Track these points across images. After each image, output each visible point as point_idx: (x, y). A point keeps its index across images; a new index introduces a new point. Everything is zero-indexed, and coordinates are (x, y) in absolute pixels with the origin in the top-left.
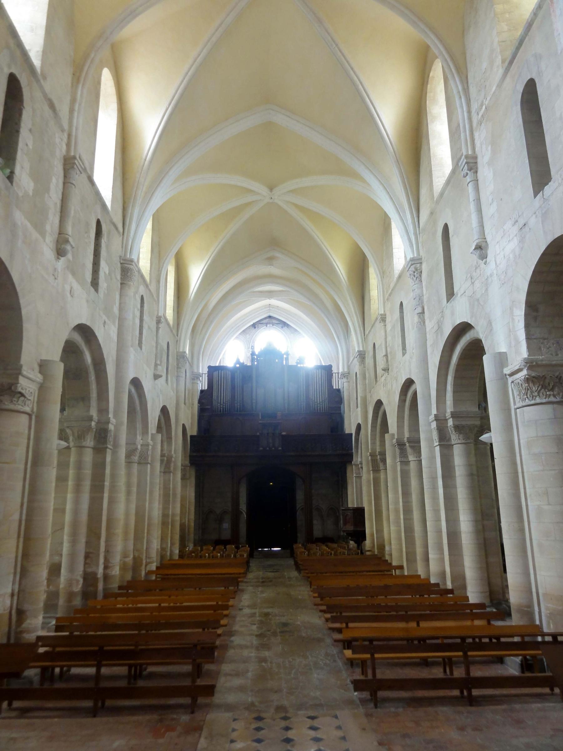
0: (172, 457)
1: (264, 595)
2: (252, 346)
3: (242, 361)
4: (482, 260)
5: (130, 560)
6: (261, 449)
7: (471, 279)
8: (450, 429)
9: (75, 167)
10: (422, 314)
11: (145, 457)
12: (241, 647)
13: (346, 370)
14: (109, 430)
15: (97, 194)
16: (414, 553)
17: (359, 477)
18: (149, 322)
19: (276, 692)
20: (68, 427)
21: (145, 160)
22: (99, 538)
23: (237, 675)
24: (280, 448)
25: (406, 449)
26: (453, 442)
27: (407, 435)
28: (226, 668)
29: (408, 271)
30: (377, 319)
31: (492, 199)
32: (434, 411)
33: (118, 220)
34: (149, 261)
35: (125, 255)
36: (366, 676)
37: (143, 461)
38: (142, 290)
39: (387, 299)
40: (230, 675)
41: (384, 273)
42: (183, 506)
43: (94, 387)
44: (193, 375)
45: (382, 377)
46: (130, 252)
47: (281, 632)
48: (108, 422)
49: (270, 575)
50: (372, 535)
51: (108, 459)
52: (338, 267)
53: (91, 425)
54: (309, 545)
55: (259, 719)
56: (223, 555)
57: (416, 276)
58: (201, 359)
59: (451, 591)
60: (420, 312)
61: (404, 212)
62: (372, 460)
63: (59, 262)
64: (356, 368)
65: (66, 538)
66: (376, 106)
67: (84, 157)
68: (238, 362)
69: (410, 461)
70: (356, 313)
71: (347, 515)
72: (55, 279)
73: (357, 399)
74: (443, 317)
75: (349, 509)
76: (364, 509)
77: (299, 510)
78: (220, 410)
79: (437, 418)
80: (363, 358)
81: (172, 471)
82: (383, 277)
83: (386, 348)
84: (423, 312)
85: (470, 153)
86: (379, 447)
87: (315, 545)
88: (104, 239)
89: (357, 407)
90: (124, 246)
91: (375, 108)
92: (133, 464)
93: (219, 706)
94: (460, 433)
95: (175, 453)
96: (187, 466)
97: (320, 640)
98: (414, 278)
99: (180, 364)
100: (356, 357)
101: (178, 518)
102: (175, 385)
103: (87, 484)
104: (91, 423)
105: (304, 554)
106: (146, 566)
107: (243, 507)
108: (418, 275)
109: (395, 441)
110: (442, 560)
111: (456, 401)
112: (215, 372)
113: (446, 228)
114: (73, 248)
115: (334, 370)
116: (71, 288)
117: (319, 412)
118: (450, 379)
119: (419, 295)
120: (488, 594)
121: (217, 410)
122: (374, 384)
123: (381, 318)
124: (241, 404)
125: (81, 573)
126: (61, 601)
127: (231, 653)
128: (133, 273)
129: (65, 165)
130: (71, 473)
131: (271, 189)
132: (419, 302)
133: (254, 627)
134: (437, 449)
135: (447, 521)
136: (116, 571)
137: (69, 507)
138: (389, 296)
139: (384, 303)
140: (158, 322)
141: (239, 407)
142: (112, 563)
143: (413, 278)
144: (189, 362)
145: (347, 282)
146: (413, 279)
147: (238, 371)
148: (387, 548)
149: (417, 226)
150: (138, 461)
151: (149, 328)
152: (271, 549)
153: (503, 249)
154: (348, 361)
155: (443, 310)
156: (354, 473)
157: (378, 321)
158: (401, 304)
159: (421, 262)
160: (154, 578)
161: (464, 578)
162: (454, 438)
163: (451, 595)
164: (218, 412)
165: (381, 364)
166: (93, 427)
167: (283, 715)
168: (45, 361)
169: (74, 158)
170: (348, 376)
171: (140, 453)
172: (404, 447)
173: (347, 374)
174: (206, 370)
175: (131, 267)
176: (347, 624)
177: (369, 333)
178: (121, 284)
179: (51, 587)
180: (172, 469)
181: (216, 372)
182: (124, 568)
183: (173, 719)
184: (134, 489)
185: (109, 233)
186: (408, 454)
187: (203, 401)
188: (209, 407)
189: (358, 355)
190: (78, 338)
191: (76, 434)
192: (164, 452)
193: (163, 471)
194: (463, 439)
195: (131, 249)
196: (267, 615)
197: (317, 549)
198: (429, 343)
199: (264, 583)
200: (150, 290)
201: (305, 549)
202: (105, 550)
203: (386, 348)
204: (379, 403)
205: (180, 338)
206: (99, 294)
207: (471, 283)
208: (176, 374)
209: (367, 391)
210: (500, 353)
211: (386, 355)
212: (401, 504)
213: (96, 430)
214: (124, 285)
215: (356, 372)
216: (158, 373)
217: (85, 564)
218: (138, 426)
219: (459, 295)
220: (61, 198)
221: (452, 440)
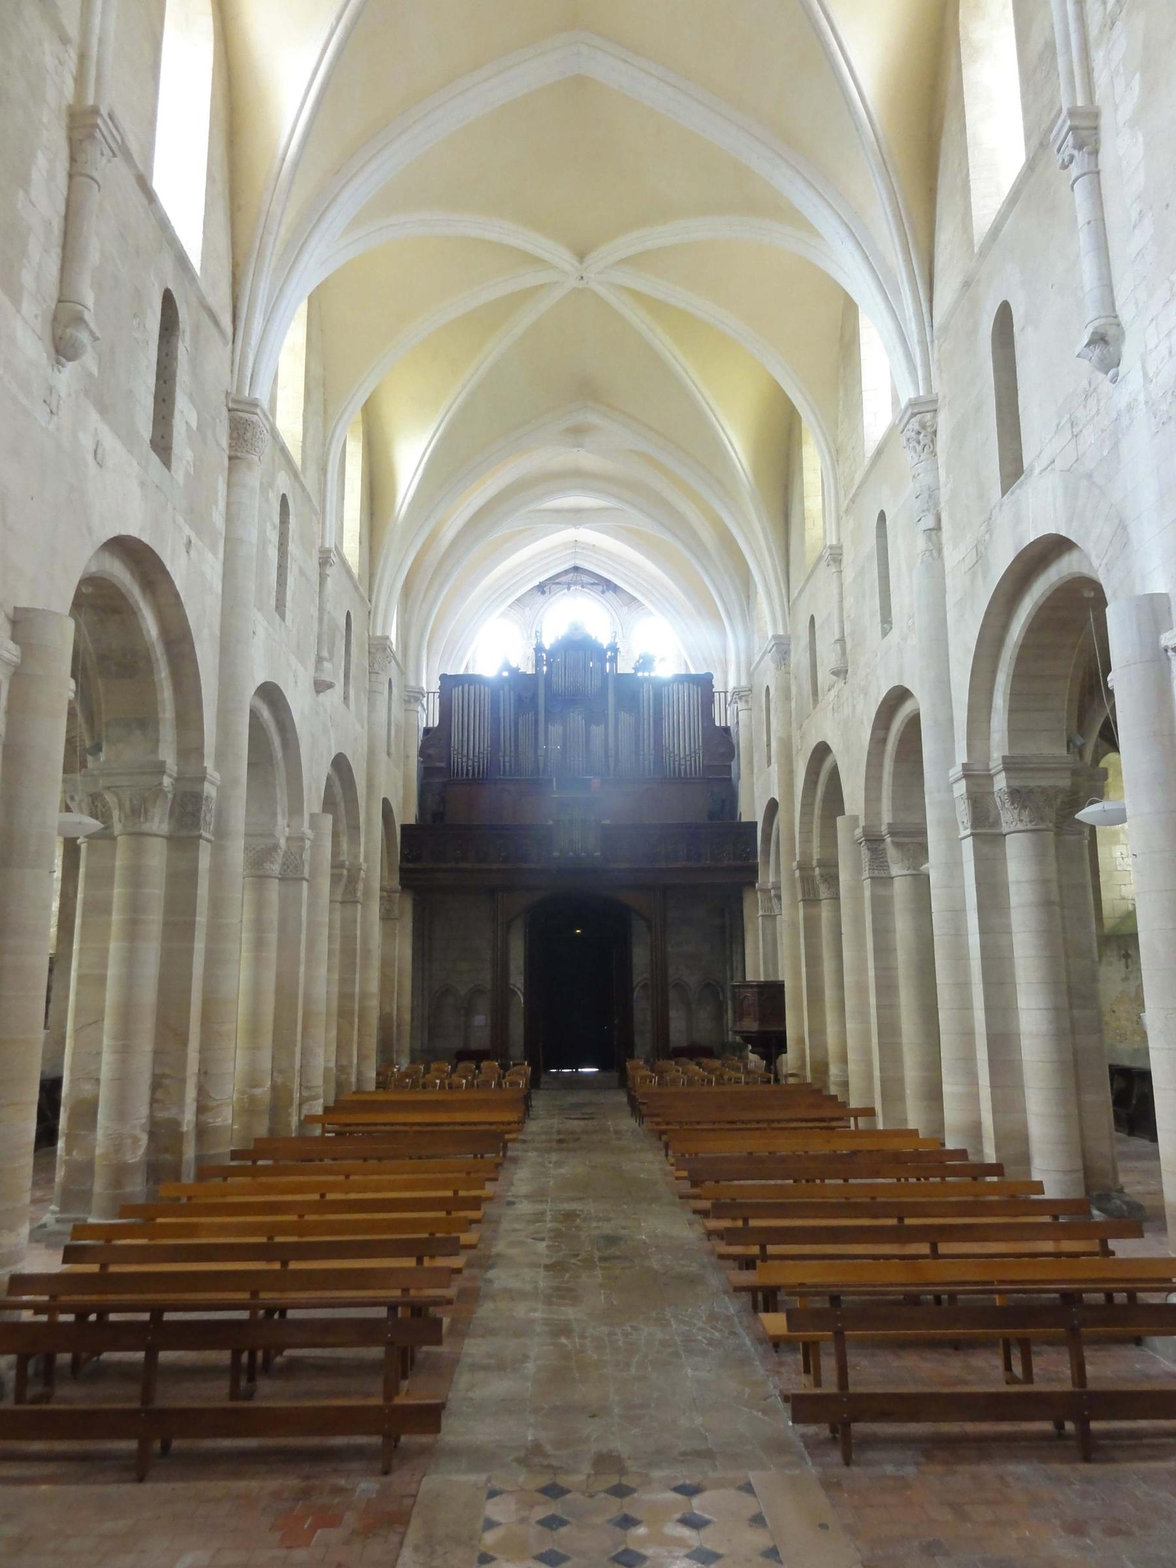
0: (361, 869)
1: (563, 1171)
2: (537, 632)
3: (514, 666)
4: (1107, 373)
5: (263, 1092)
6: (556, 854)
7: (1072, 425)
8: (1000, 797)
9: (98, 135)
10: (935, 532)
11: (296, 865)
12: (511, 1295)
13: (744, 683)
14: (205, 794)
15: (163, 225)
16: (900, 1081)
17: (771, 918)
18: (301, 559)
19: (593, 1416)
20: (108, 788)
21: (283, 160)
22: (185, 1043)
23: (501, 1367)
25: (884, 849)
26: (1005, 829)
27: (886, 818)
28: (474, 1348)
29: (902, 432)
30: (820, 558)
31: (1141, 211)
32: (961, 757)
33: (220, 300)
34: (301, 420)
35: (239, 389)
36: (818, 1383)
37: (291, 876)
38: (283, 483)
39: (847, 511)
40: (485, 1368)
41: (836, 453)
42: (385, 979)
43: (167, 695)
44: (406, 693)
45: (829, 690)
46: (251, 385)
47: (602, 1259)
48: (202, 778)
49: (577, 1125)
50: (801, 1041)
51: (204, 862)
52: (731, 444)
53: (161, 784)
54: (662, 1063)
55: (554, 1491)
56: (474, 1084)
57: (922, 443)
58: (424, 658)
59: (997, 1169)
60: (931, 527)
61: (898, 292)
62: (802, 878)
63: (60, 371)
64: (769, 677)
65: (106, 1041)
66: (835, 22)
67: (126, 124)
68: (507, 667)
69: (892, 878)
70: (770, 550)
71: (746, 997)
72: (52, 412)
73: (769, 745)
74: (989, 531)
75: (748, 985)
76: (783, 986)
77: (638, 988)
78: (467, 770)
79: (968, 773)
80: (785, 653)
81: (361, 900)
82: (838, 461)
83: (842, 622)
84: (938, 528)
85: (1080, 103)
86: (819, 849)
87: (674, 1063)
88: (183, 341)
89: (769, 763)
90: (236, 366)
91: (833, 28)
92: (271, 879)
93: (454, 1453)
94: (1024, 807)
95: (366, 859)
96: (395, 892)
97: (692, 1281)
98: (917, 445)
99: (376, 665)
100: (768, 650)
101: (374, 1003)
102: (365, 714)
103: (155, 919)
104: (162, 778)
105: (651, 1082)
106: (300, 1105)
107: (517, 980)
108: (927, 441)
109: (859, 832)
110: (974, 1098)
111: (1015, 732)
113: (1004, 314)
114: (96, 339)
115: (718, 686)
116: (98, 444)
118: (1002, 680)
119: (929, 488)
120: (1081, 1175)
121: (460, 771)
122: (812, 707)
123: (831, 554)
124: (513, 758)
125: (144, 1121)
126: (99, 1186)
127: (485, 1310)
128: (259, 433)
129: (71, 128)
130: (118, 892)
131: (581, 256)
132: (928, 502)
133: (542, 1246)
134: (968, 846)
135: (989, 1009)
136: (225, 1118)
137: (113, 971)
138: (851, 503)
139: (838, 519)
140: (324, 562)
142: (216, 1100)
143: (914, 447)
144: (398, 664)
145: (751, 478)
146: (916, 452)
147: (506, 688)
148: (834, 1070)
149: (926, 324)
150: (280, 874)
151: (302, 572)
153: (1168, 335)
154: (749, 663)
155: (991, 513)
156: (760, 908)
157: (823, 564)
158: (882, 516)
159: (934, 408)
160: (318, 1132)
161: (1025, 1139)
162: (1009, 818)
163: (995, 1179)
164: (462, 774)
165: (828, 658)
166: (165, 789)
167: (614, 1480)
168: (26, 610)
169: (95, 111)
171: (284, 855)
172: (879, 846)
174: (435, 686)
175: (255, 418)
176: (763, 1248)
177: (800, 594)
178: (230, 458)
179: (75, 1153)
180: (359, 894)
182: (249, 1108)
183: (337, 1491)
184: (273, 937)
185: (197, 330)
186: (889, 861)
187: (431, 751)
188: (443, 765)
189: (773, 646)
190: (119, 572)
191: (127, 804)
192: (342, 858)
193: (340, 900)
194: (1031, 821)
195: (252, 375)
196: (570, 1216)
197: (678, 1071)
198: (951, 600)
199: (564, 1142)
200: (303, 489)
201: (652, 1071)
202: (199, 1070)
203: (842, 622)
204: (822, 751)
205: (376, 607)
206: (172, 472)
207: (1070, 437)
208: (367, 687)
209: (794, 725)
210: (1152, 597)
211: (842, 640)
212: (871, 973)
213: (175, 796)
214: (236, 461)
215: (768, 687)
216: (326, 677)
217: (153, 1101)
218: (279, 796)
219: (1037, 471)
220: (63, 214)
221: (1004, 825)
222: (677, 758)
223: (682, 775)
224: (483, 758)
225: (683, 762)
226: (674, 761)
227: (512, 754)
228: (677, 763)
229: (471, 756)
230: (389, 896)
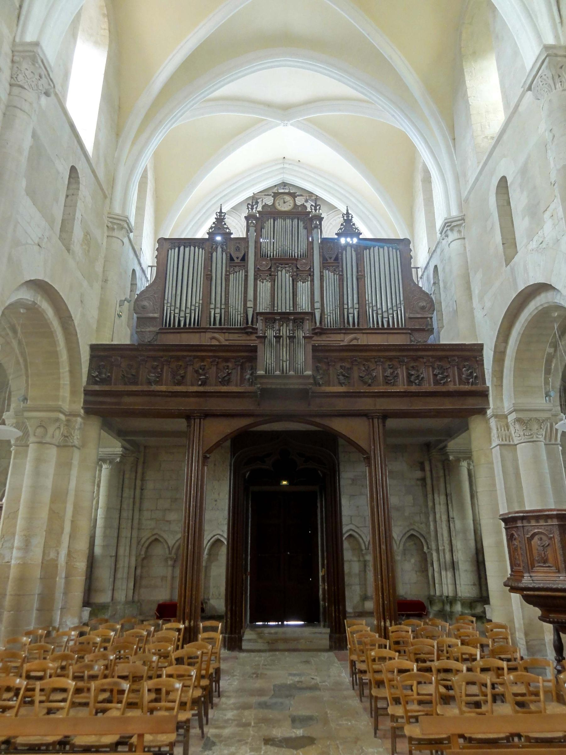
6: (261, 372)
24: (309, 373)
44: (111, 220)
80: (561, 67)
96: (77, 415)
99: (20, 77)
112: (171, 249)
117: (386, 326)
124: (223, 311)
141: (218, 316)
152: (283, 622)
170: (460, 225)
173: (459, 220)
181: (173, 250)
187: (145, 303)
188: (156, 315)
205: (28, 12)
222: (380, 312)
223: (386, 326)
224: (195, 310)
225: (385, 315)
226: (377, 314)
227: (223, 307)
228: (380, 316)
229: (183, 308)
230: (68, 421)
